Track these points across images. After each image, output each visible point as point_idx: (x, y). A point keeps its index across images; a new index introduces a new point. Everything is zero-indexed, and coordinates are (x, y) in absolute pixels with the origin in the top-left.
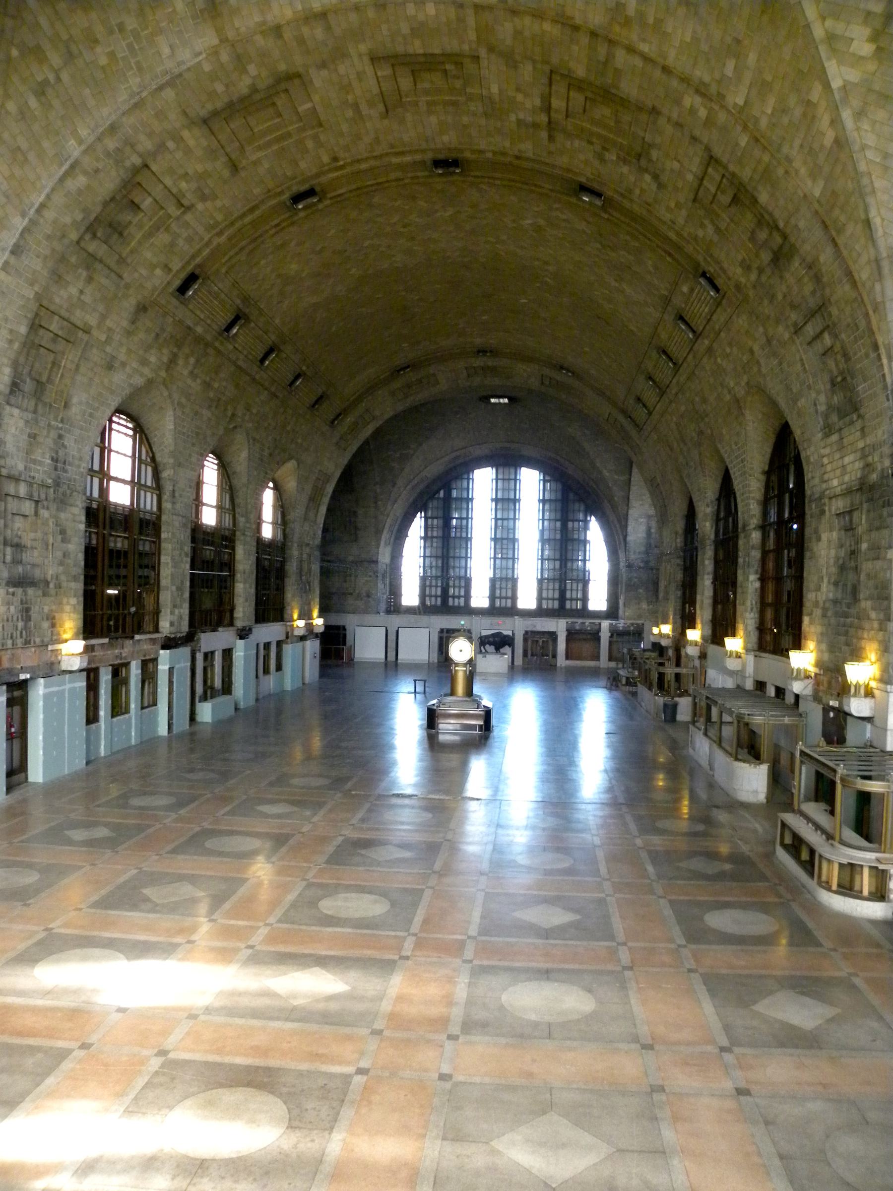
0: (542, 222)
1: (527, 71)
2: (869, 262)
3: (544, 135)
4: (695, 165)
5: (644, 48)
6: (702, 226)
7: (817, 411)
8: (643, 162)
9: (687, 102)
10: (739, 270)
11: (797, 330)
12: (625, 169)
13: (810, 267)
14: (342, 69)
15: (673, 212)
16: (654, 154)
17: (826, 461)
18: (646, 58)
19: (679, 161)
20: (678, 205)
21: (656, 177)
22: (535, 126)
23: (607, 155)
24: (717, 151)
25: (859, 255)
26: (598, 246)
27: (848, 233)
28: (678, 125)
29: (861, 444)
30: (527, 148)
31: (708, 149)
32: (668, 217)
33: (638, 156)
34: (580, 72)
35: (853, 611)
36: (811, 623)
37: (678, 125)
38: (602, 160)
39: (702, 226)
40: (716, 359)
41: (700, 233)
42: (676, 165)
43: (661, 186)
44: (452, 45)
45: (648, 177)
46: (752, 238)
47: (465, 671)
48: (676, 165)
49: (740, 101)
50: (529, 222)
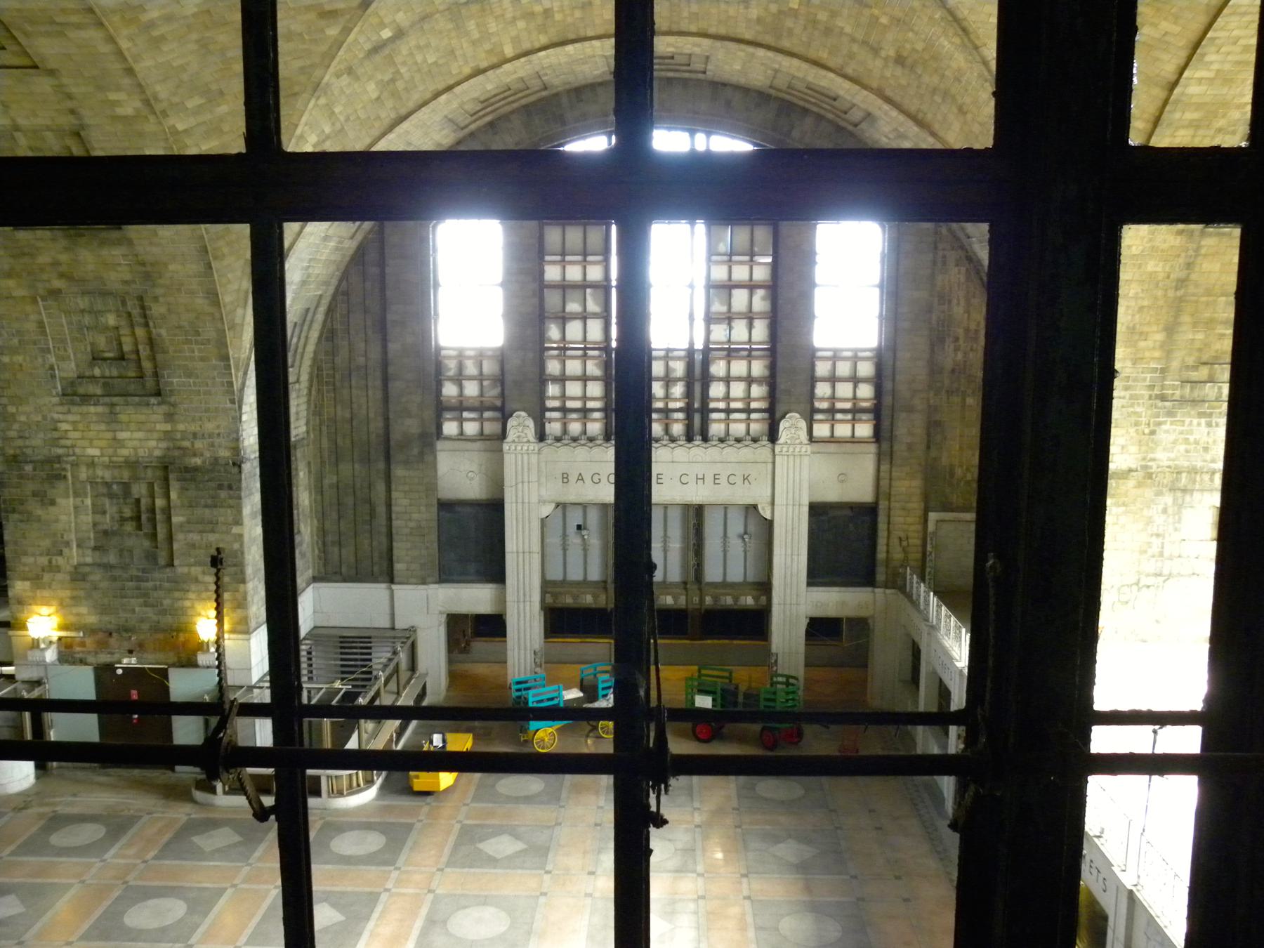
2: (238, 290)
5: (124, 44)
7: (53, 376)
17: (64, 426)
18: (120, 53)
25: (229, 282)
27: (225, 262)
29: (168, 427)
49: (180, 127)
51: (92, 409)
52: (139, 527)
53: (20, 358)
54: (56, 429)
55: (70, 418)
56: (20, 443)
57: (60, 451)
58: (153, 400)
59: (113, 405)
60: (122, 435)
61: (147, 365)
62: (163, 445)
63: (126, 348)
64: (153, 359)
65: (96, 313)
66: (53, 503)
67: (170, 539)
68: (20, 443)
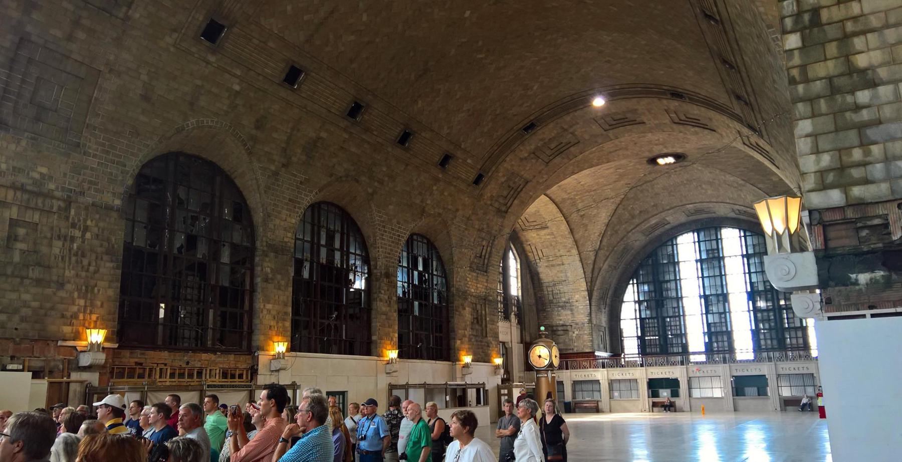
0: (530, 93)
1: (587, 137)
3: (566, 127)
4: (527, 176)
6: (504, 176)
9: (545, 176)
10: (489, 195)
11: (480, 230)
12: (533, 147)
14: (657, 122)
15: (509, 163)
16: (534, 161)
20: (512, 165)
21: (526, 158)
22: (571, 127)
23: (541, 143)
24: (529, 184)
26: (498, 112)
28: (540, 172)
30: (568, 118)
32: (508, 159)
33: (535, 154)
34: (572, 149)
35: (484, 340)
36: (462, 343)
38: (542, 140)
39: (504, 176)
41: (500, 174)
43: (521, 159)
44: (616, 131)
45: (526, 155)
46: (499, 196)
50: (535, 88)
52: (478, 322)
65: (483, 239)
67: (486, 326)
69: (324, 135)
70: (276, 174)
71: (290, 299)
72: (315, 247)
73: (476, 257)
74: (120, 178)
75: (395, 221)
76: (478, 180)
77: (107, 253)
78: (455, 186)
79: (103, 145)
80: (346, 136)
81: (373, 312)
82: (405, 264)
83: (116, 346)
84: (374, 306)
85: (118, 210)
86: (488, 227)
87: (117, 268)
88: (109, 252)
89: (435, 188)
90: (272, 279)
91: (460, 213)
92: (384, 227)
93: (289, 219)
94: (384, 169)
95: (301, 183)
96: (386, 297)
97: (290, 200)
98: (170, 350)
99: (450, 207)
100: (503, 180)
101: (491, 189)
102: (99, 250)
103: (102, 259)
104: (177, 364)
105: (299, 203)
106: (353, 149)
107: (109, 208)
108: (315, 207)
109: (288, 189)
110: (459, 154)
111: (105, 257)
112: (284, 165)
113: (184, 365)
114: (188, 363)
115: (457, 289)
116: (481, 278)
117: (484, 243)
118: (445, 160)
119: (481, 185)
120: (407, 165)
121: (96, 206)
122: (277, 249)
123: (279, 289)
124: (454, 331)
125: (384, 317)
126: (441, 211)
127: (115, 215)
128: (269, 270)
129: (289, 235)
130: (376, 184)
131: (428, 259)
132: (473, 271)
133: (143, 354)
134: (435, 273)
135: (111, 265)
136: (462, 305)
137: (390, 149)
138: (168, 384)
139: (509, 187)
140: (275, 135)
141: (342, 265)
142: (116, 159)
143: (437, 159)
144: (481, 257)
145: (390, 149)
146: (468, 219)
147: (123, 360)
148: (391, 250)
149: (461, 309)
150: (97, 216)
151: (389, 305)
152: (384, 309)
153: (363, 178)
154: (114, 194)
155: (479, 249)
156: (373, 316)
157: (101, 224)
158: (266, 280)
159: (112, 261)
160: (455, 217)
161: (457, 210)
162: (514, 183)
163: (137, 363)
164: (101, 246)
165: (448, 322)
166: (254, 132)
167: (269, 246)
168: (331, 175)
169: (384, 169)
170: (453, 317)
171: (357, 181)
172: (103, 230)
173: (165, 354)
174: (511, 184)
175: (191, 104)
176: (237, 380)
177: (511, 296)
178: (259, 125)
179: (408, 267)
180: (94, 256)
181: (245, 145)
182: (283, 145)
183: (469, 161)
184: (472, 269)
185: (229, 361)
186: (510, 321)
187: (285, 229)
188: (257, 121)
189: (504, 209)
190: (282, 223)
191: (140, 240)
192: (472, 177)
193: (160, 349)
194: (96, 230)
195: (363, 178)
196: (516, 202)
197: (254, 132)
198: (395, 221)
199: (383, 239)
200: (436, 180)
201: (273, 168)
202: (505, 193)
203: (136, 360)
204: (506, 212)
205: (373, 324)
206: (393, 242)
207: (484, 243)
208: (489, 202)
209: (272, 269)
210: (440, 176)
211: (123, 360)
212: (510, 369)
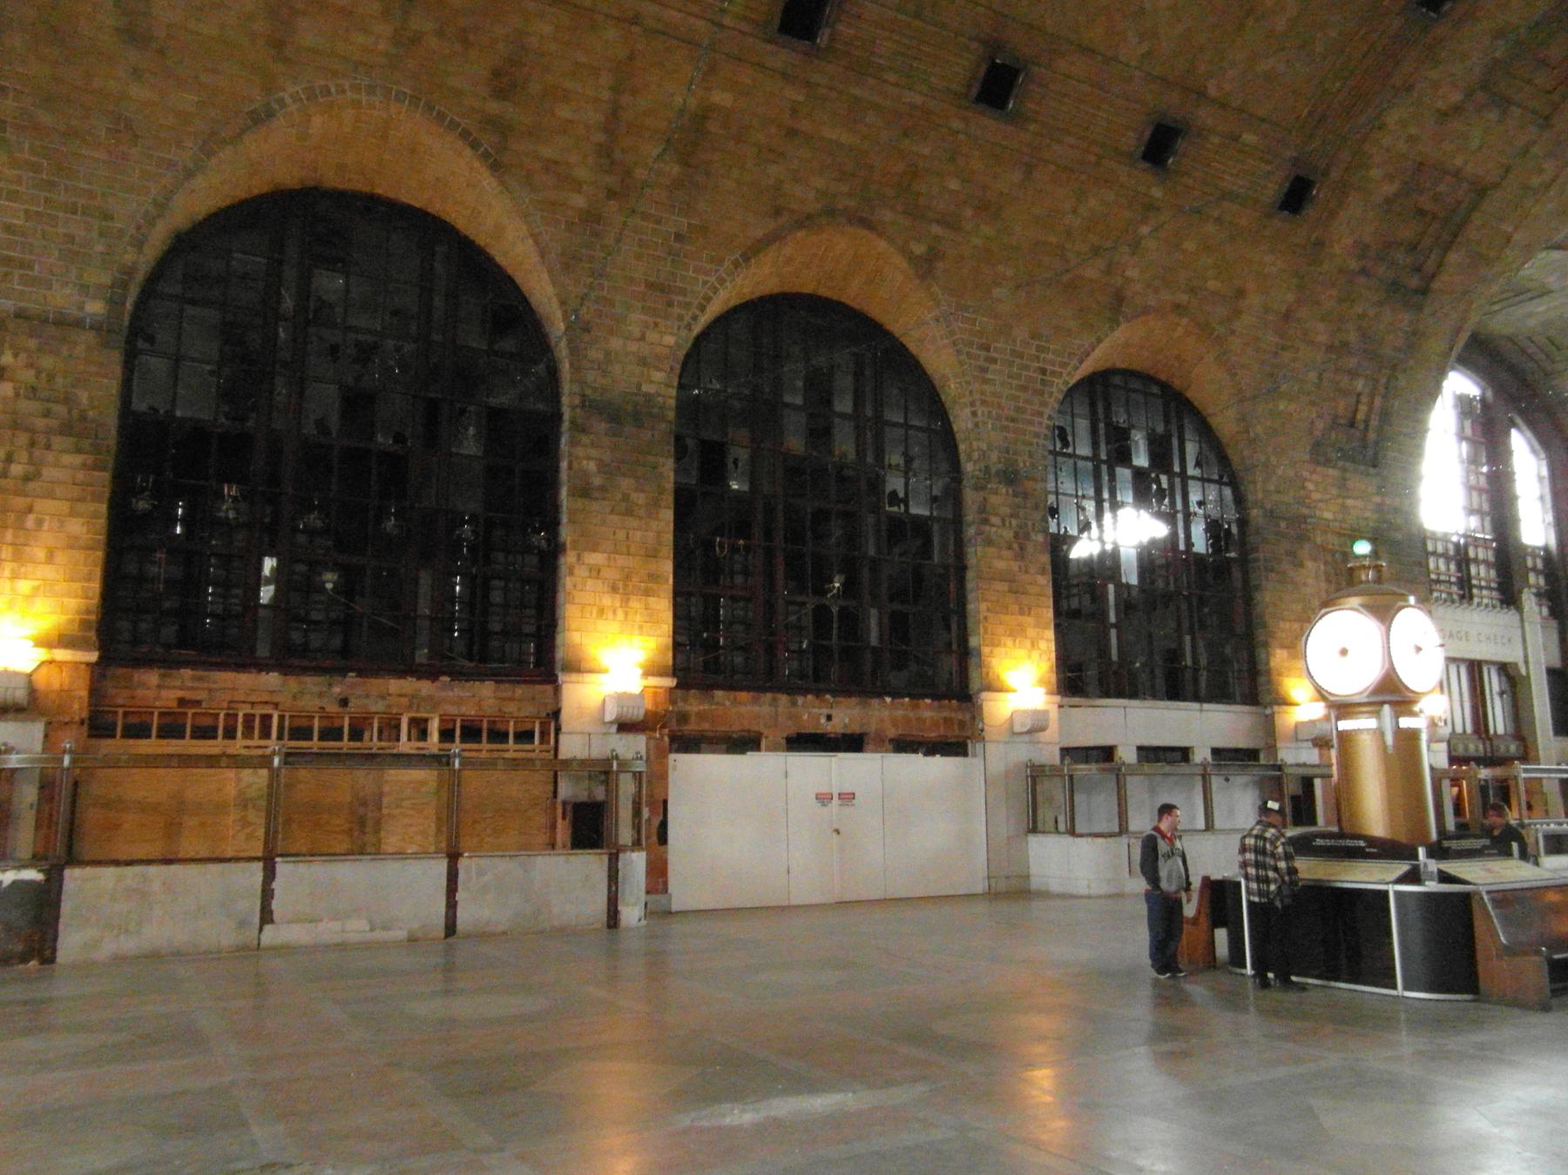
8: (1480, 95)
13: (1414, 334)
16: (1493, 115)
17: (1310, 486)
19: (1480, 148)
20: (1412, 139)
21: (1457, 109)
28: (1525, 151)
31: (1496, 186)
37: (1525, 151)
38: (1500, 34)
40: (1145, 220)
41: (1375, 173)
42: (1475, 143)
43: (1443, 115)
45: (1457, 97)
47: (1379, 733)
48: (1475, 143)
51: (1331, 471)
53: (1292, 407)
54: (1304, 488)
55: (1314, 477)
56: (1275, 497)
57: (1305, 511)
58: (1372, 471)
59: (1345, 470)
60: (1349, 502)
61: (1372, 436)
62: (1375, 516)
63: (1360, 416)
64: (1380, 430)
65: (1353, 374)
66: (1301, 565)
68: (1275, 497)
69: (722, 98)
70: (592, 219)
71: (669, 538)
72: (763, 415)
73: (1334, 424)
74: (99, 248)
75: (1021, 333)
76: (1296, 197)
77: (66, 429)
78: (1218, 220)
79: (35, 168)
80: (794, 94)
81: (970, 575)
82: (1084, 449)
83: (93, 657)
84: (972, 560)
85: (96, 327)
86: (1364, 335)
87: (96, 467)
88: (75, 428)
89: (1145, 230)
90: (603, 488)
91: (1254, 300)
92: (988, 350)
93: (652, 336)
94: (954, 185)
95: (679, 237)
96: (1008, 534)
97: (651, 286)
98: (285, 669)
99: (1212, 285)
100: (1390, 189)
101: (1351, 224)
102: (40, 423)
103: (48, 447)
104: (310, 703)
105: (683, 292)
106: (831, 134)
107: (67, 323)
108: (769, 316)
109: (639, 257)
110: (1204, 116)
111: (58, 442)
112: (611, 194)
113: (333, 708)
114: (344, 702)
115: (1271, 515)
116: (1356, 482)
117: (1360, 385)
118: (1160, 145)
119: (1310, 212)
120: (1029, 170)
121: (27, 318)
122: (620, 414)
123: (629, 512)
124: (1265, 626)
125: (1003, 587)
126: (1183, 298)
127: (89, 337)
128: (592, 466)
129: (658, 376)
130: (936, 229)
131: (1167, 437)
132: (1328, 462)
133: (200, 679)
134: (1192, 471)
135: (77, 460)
136: (1291, 554)
137: (956, 124)
138: (484, 755)
139: (1421, 212)
140: (564, 112)
141: (861, 453)
142: (82, 201)
143: (1133, 140)
144: (1352, 424)
145: (956, 124)
146: (1287, 316)
147: (140, 693)
148: (1018, 409)
149: (1285, 565)
150: (32, 343)
151: (1021, 554)
152: (1000, 565)
153: (887, 215)
154: (84, 288)
155: (1342, 406)
156: (970, 585)
157: (47, 362)
158: (583, 491)
159: (79, 451)
160: (1237, 313)
161: (1241, 293)
162: (1436, 198)
163: (182, 702)
164: (47, 414)
165: (1249, 601)
166: (494, 107)
167: (587, 404)
168: (777, 212)
169: (954, 185)
170: (1257, 588)
171: (867, 224)
172: (51, 377)
173: (272, 679)
174: (1426, 202)
175: (278, 45)
176: (485, 745)
177: (1523, 551)
178: (504, 83)
179: (1095, 458)
180: (23, 439)
181: (474, 145)
182: (599, 137)
183: (1249, 138)
184: (1319, 455)
185: (481, 698)
186: (1519, 609)
187: (643, 362)
188: (496, 73)
189: (1415, 282)
190: (633, 347)
191: (195, 403)
192: (1273, 188)
193: (261, 667)
194: (28, 376)
195: (887, 215)
196: (1454, 257)
197: (494, 107)
198: (1021, 333)
199: (985, 381)
200: (1150, 207)
201: (579, 201)
202: (1407, 233)
203: (180, 694)
204: (1424, 291)
205: (971, 607)
206: (1024, 388)
207: (1360, 385)
208: (1353, 265)
209: (601, 465)
210: (1157, 193)
211: (140, 693)
212: (1525, 733)
